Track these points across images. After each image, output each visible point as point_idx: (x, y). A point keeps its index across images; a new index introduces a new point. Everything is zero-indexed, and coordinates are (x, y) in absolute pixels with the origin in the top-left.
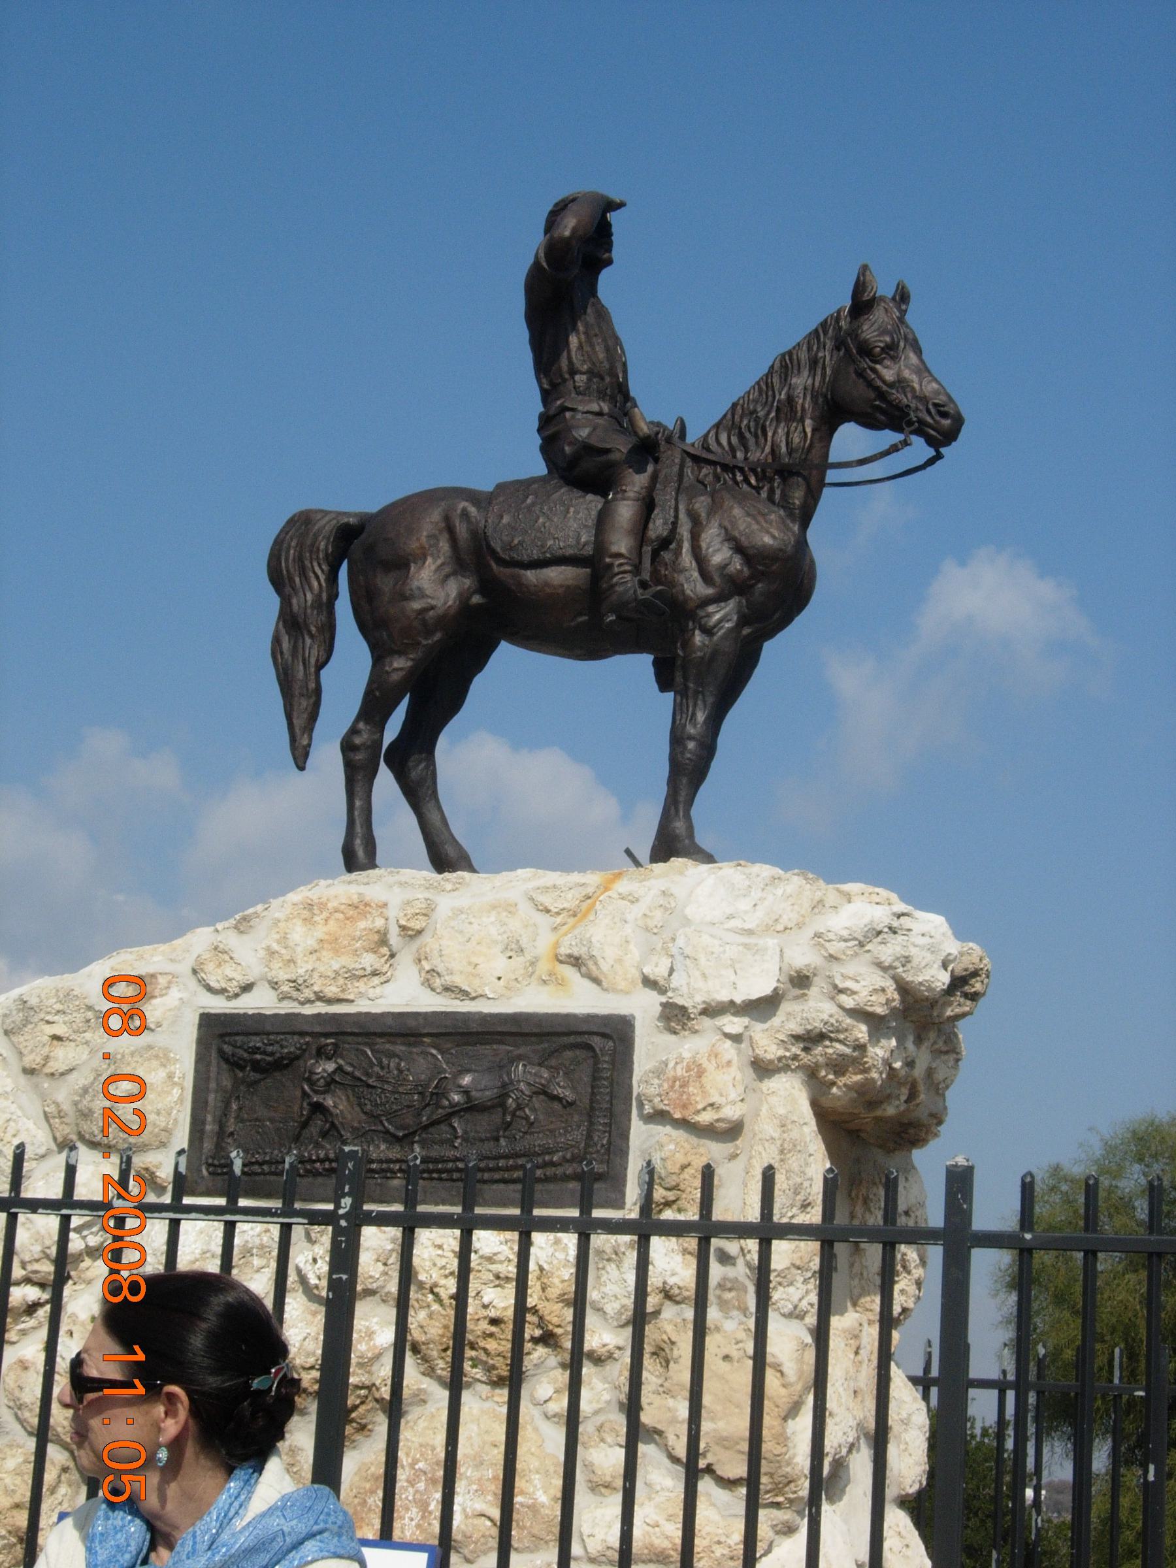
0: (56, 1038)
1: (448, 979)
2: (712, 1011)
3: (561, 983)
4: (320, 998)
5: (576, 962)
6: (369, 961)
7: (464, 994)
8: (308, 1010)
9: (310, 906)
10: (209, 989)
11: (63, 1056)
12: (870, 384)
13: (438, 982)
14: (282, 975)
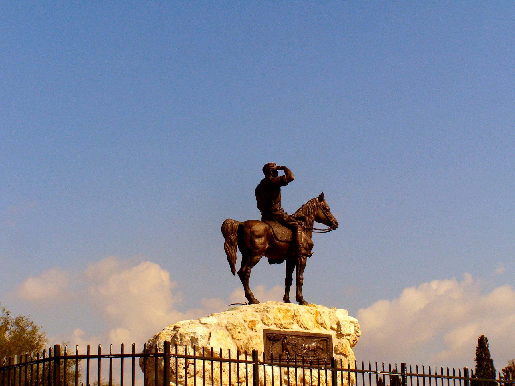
0: (239, 332)
1: (305, 326)
2: (347, 335)
3: (319, 328)
4: (284, 328)
5: (321, 324)
6: (291, 321)
7: (307, 329)
8: (282, 330)
9: (279, 309)
10: (265, 324)
11: (240, 336)
12: (326, 216)
13: (302, 326)
14: (279, 323)
